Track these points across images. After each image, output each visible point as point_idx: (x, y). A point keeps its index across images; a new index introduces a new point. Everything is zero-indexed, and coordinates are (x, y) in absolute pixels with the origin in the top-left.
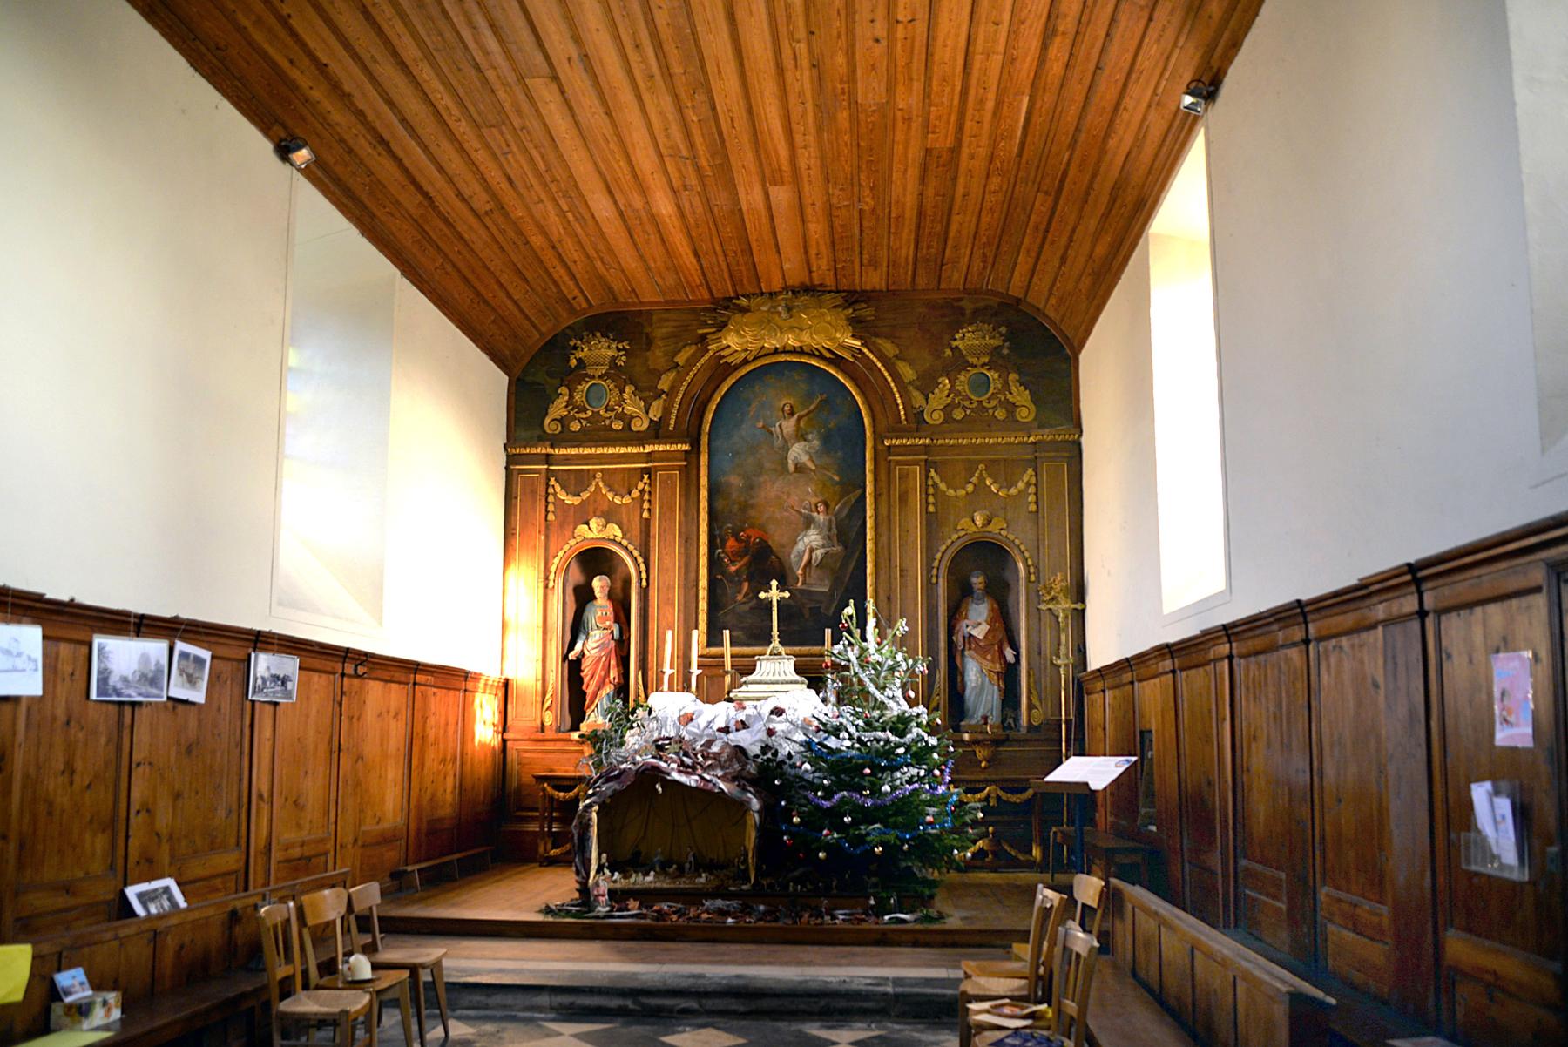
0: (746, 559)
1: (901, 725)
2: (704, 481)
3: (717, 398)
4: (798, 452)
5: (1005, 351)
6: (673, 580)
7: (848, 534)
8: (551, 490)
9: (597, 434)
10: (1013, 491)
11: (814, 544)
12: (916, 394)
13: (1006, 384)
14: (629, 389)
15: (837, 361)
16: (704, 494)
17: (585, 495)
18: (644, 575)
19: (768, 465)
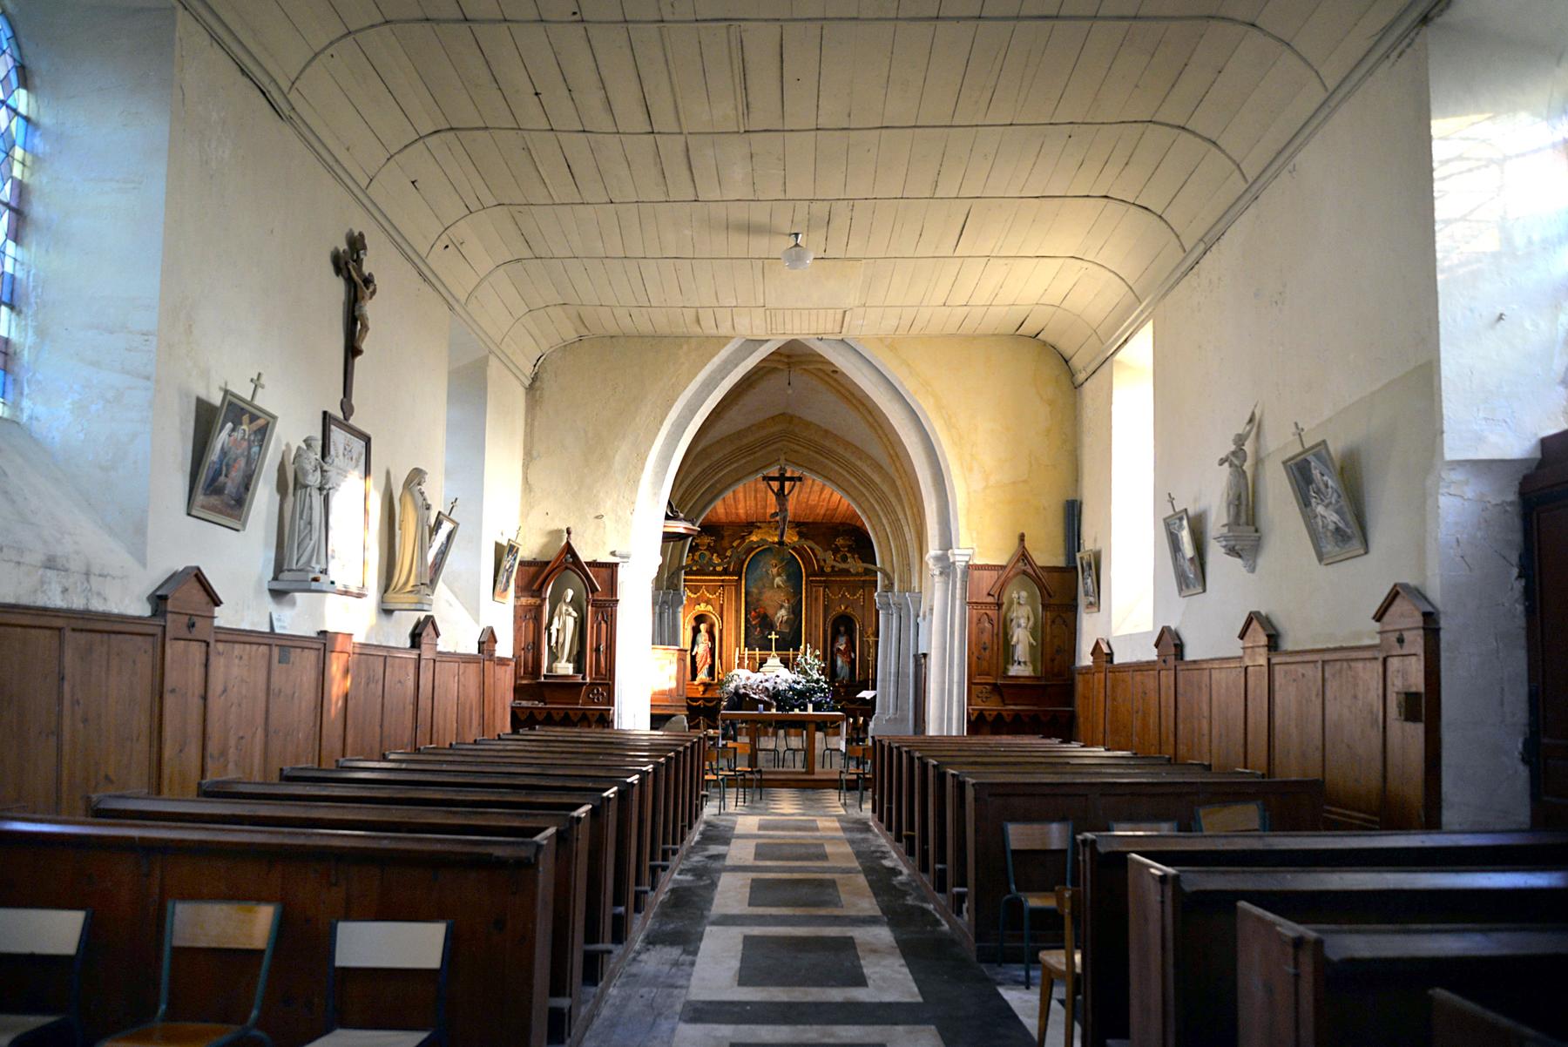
1: (817, 681)
4: (778, 580)
6: (732, 628)
7: (796, 611)
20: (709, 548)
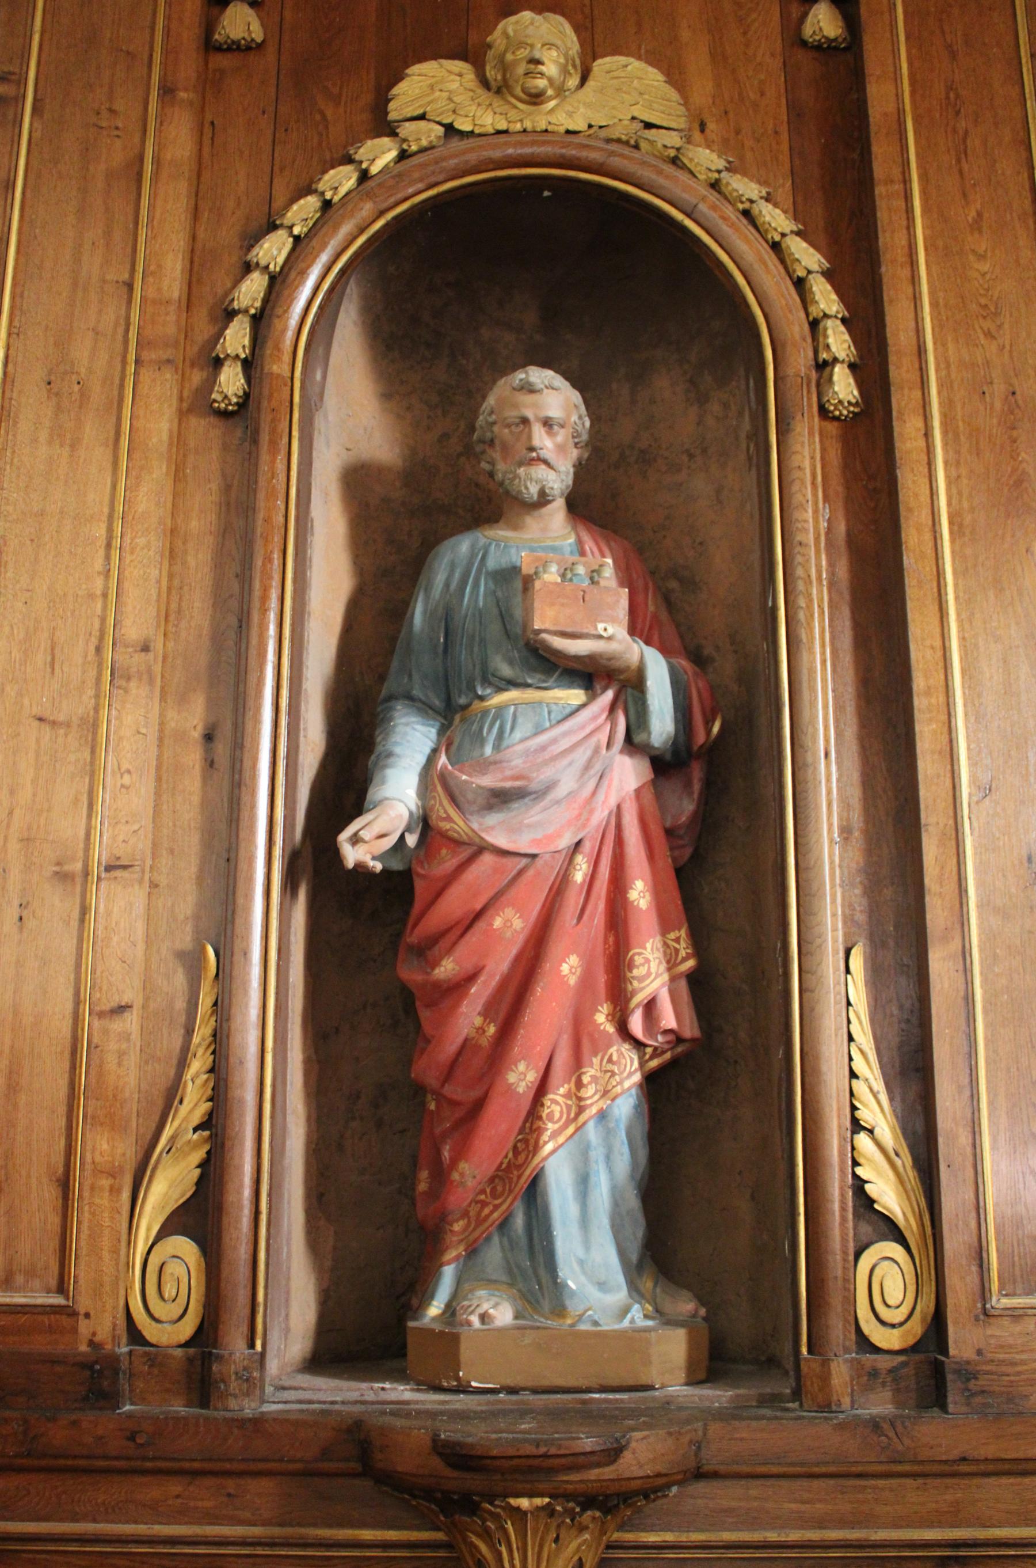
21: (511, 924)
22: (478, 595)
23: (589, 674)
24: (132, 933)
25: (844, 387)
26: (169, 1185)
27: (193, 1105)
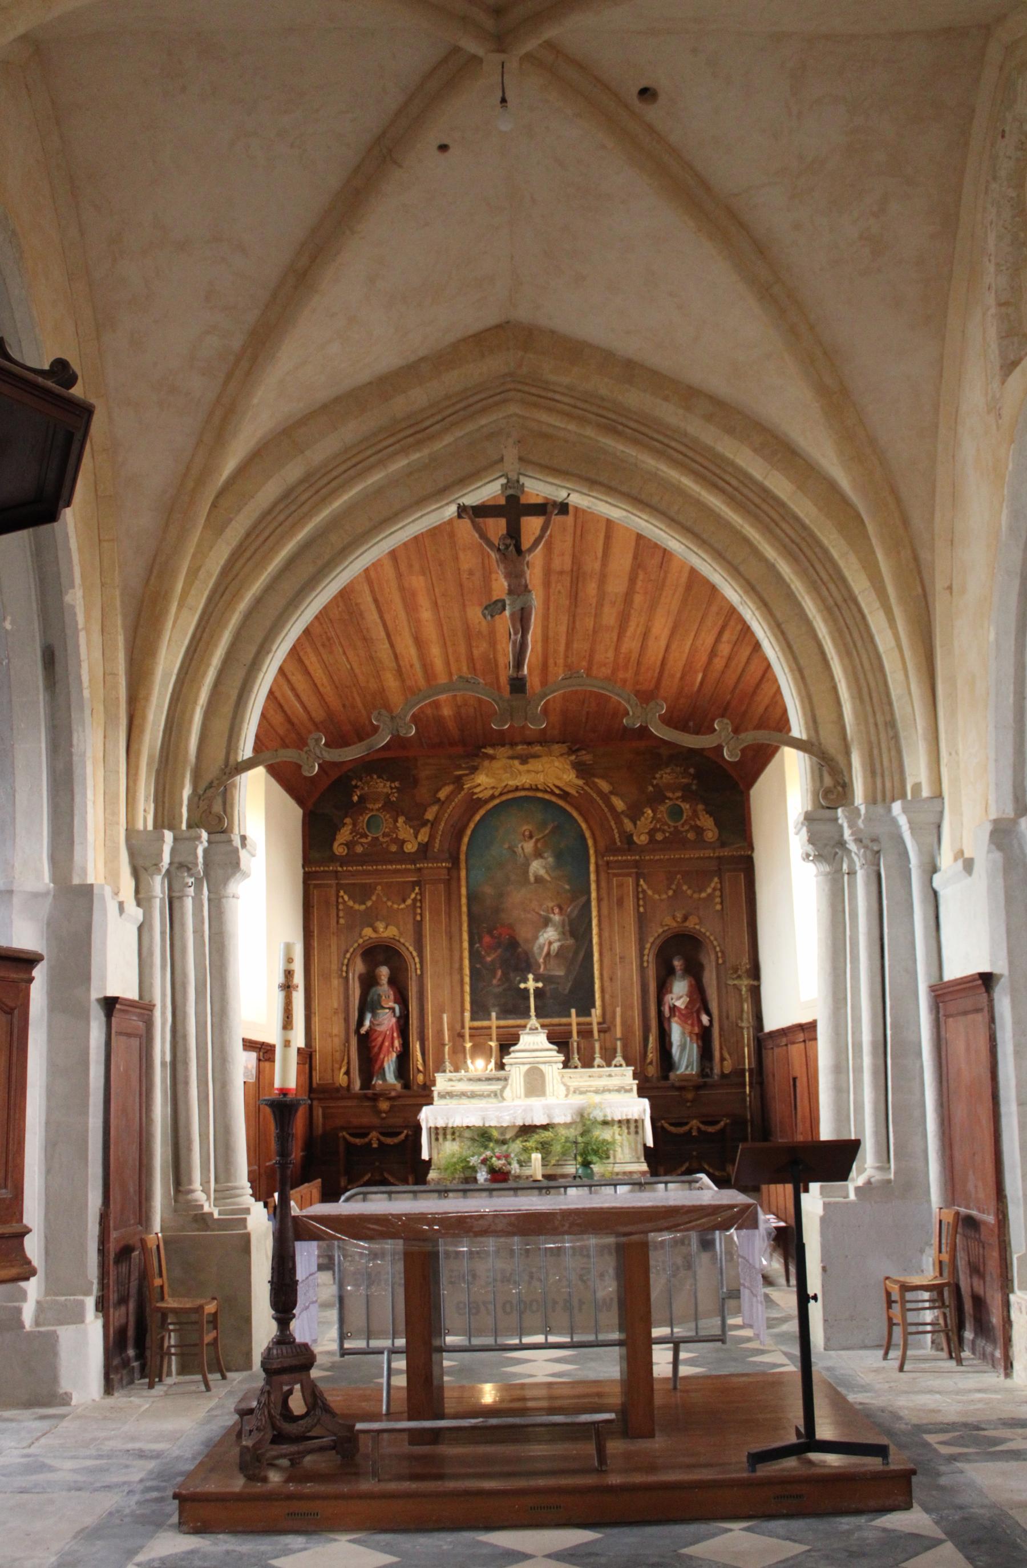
0: (499, 951)
2: (464, 891)
3: (472, 825)
4: (537, 867)
5: (694, 787)
8: (340, 900)
9: (377, 855)
10: (703, 895)
11: (552, 938)
12: (626, 821)
13: (695, 811)
14: (401, 820)
15: (565, 795)
16: (464, 901)
17: (369, 903)
18: (418, 966)
19: (513, 877)
20: (389, 806)
21: (380, 1039)
22: (376, 997)
23: (389, 1008)
24: (337, 1042)
25: (419, 972)
26: (343, 1070)
27: (346, 1061)
